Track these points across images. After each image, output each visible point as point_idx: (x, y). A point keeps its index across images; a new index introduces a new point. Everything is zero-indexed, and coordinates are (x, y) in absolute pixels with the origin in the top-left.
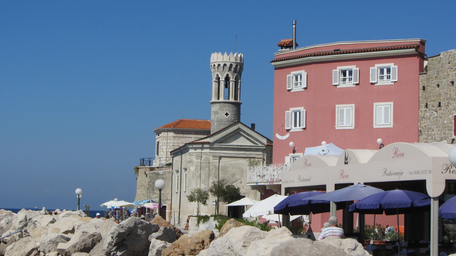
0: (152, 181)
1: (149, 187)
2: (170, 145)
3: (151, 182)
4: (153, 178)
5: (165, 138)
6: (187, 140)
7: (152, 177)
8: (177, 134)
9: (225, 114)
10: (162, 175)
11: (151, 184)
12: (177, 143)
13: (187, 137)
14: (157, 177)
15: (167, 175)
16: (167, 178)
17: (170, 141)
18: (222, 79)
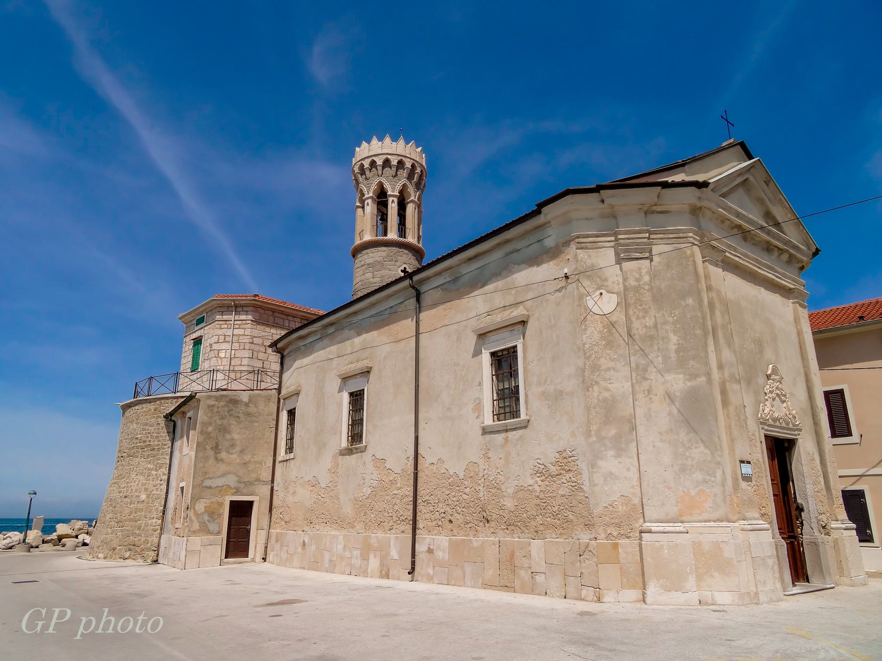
1: (204, 439)
3: (210, 424)
10: (247, 405)
11: (210, 433)
14: (232, 410)
15: (261, 406)
16: (260, 414)
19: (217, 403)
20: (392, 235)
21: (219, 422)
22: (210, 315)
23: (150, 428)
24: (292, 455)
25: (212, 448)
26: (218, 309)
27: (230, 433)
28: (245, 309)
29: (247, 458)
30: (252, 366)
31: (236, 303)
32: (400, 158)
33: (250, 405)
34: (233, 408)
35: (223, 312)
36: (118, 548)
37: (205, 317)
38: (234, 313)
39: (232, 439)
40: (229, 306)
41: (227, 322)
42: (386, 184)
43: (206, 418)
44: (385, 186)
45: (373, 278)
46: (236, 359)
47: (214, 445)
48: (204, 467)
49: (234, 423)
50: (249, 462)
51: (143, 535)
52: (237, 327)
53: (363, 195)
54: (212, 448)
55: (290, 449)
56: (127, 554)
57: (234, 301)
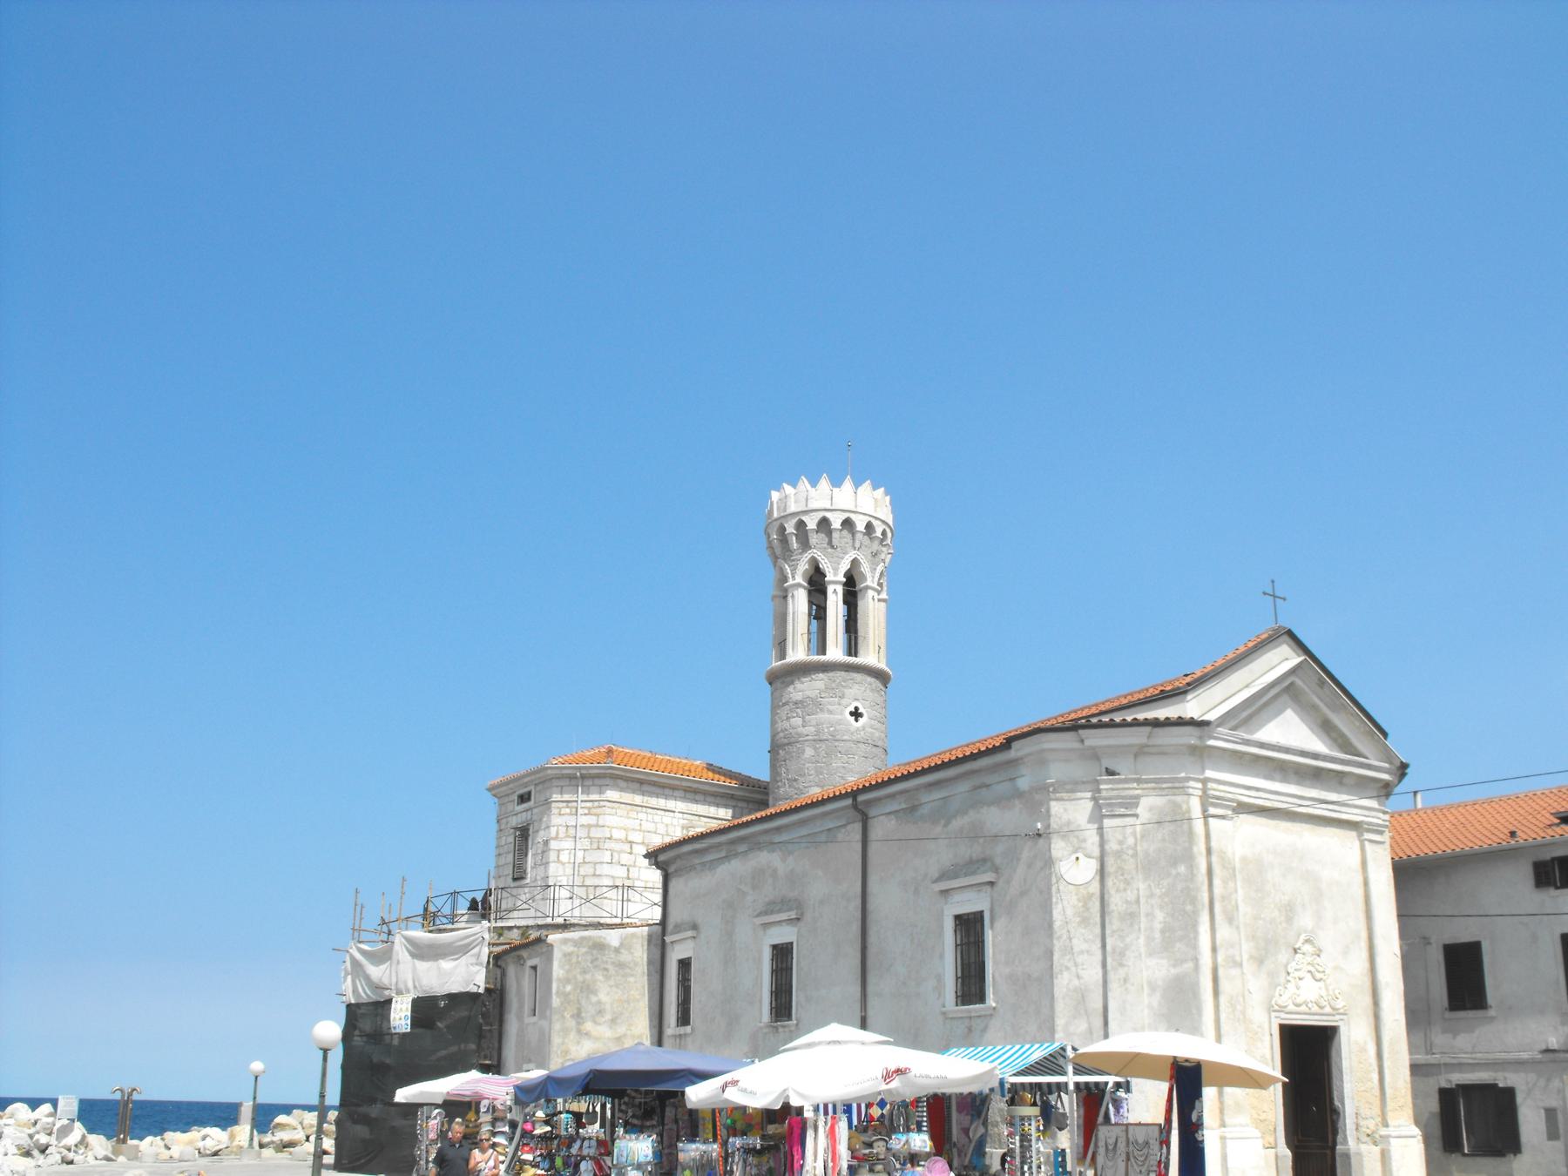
0: (575, 978)
2: (591, 835)
4: (578, 962)
5: (568, 807)
6: (657, 819)
7: (574, 960)
8: (622, 793)
9: (852, 714)
10: (617, 950)
11: (569, 994)
12: (621, 828)
13: (658, 809)
14: (597, 959)
17: (595, 818)
18: (835, 575)
19: (576, 949)
20: (835, 651)
21: (580, 978)
22: (540, 791)
24: (688, 1029)
25: (572, 1016)
26: (555, 782)
27: (595, 992)
28: (597, 781)
29: (621, 1030)
30: (612, 877)
31: (584, 772)
32: (846, 515)
33: (622, 951)
34: (599, 956)
35: (562, 787)
37: (533, 794)
38: (580, 788)
39: (599, 1002)
40: (571, 777)
41: (570, 805)
42: (823, 562)
43: (562, 972)
44: (821, 566)
45: (804, 727)
46: (588, 865)
47: (575, 1011)
48: (563, 1043)
49: (601, 978)
50: (625, 1035)
52: (586, 811)
53: (785, 579)
54: (572, 1016)
55: (684, 1019)
57: (580, 768)
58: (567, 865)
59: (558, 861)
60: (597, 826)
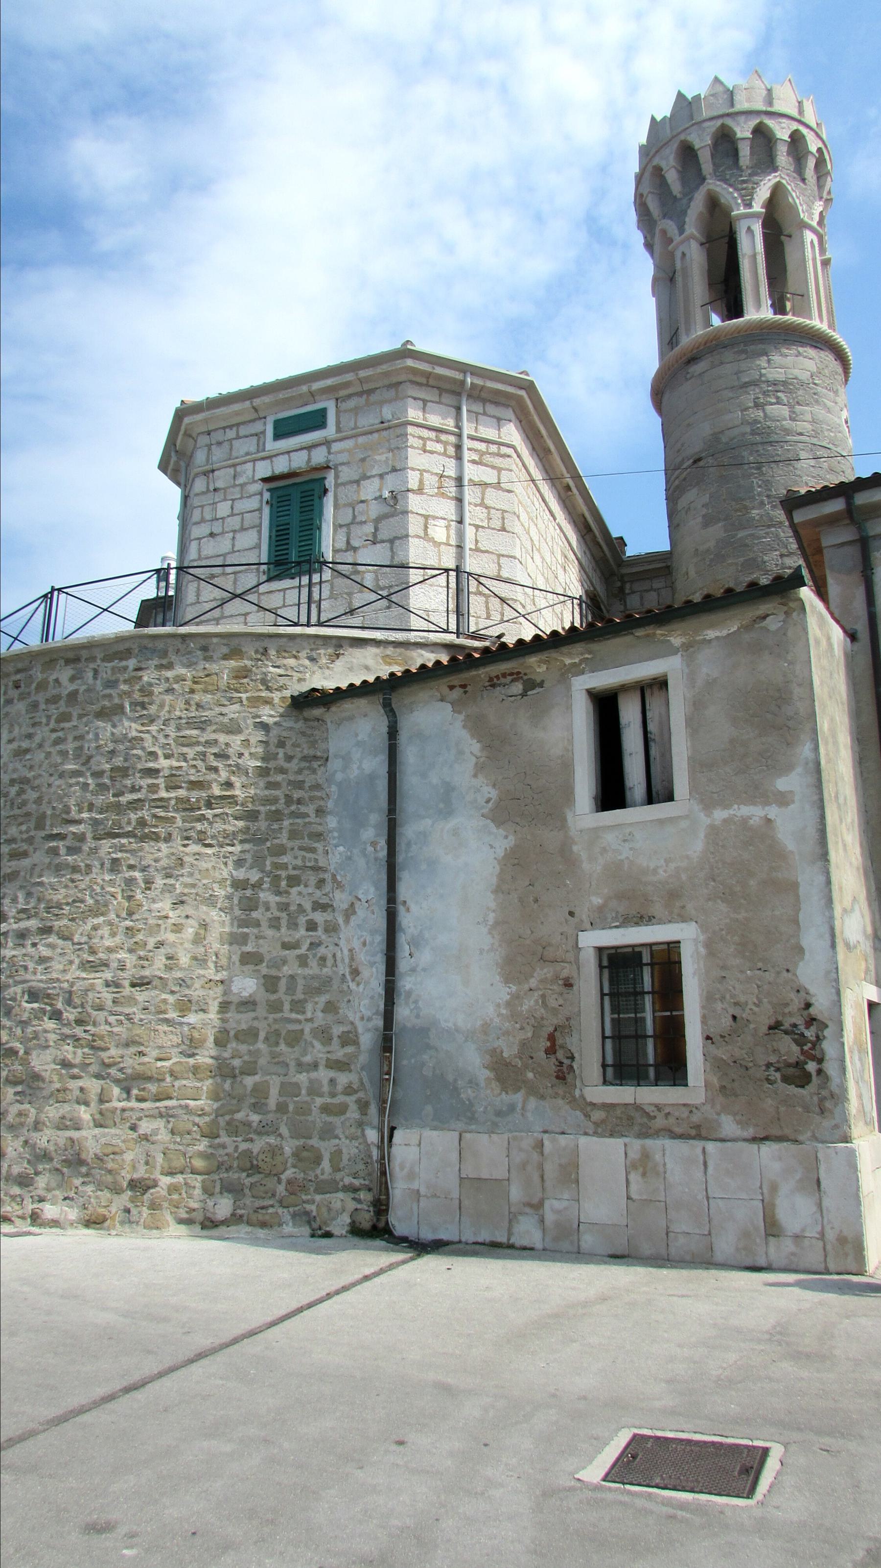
2: (488, 502)
5: (438, 441)
23: (222, 738)
36: (165, 1181)
51: (284, 1130)
56: (223, 1207)
58: (443, 547)
59: (426, 537)
60: (498, 486)
